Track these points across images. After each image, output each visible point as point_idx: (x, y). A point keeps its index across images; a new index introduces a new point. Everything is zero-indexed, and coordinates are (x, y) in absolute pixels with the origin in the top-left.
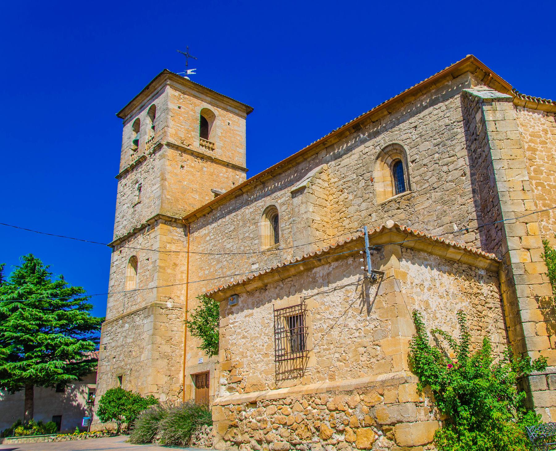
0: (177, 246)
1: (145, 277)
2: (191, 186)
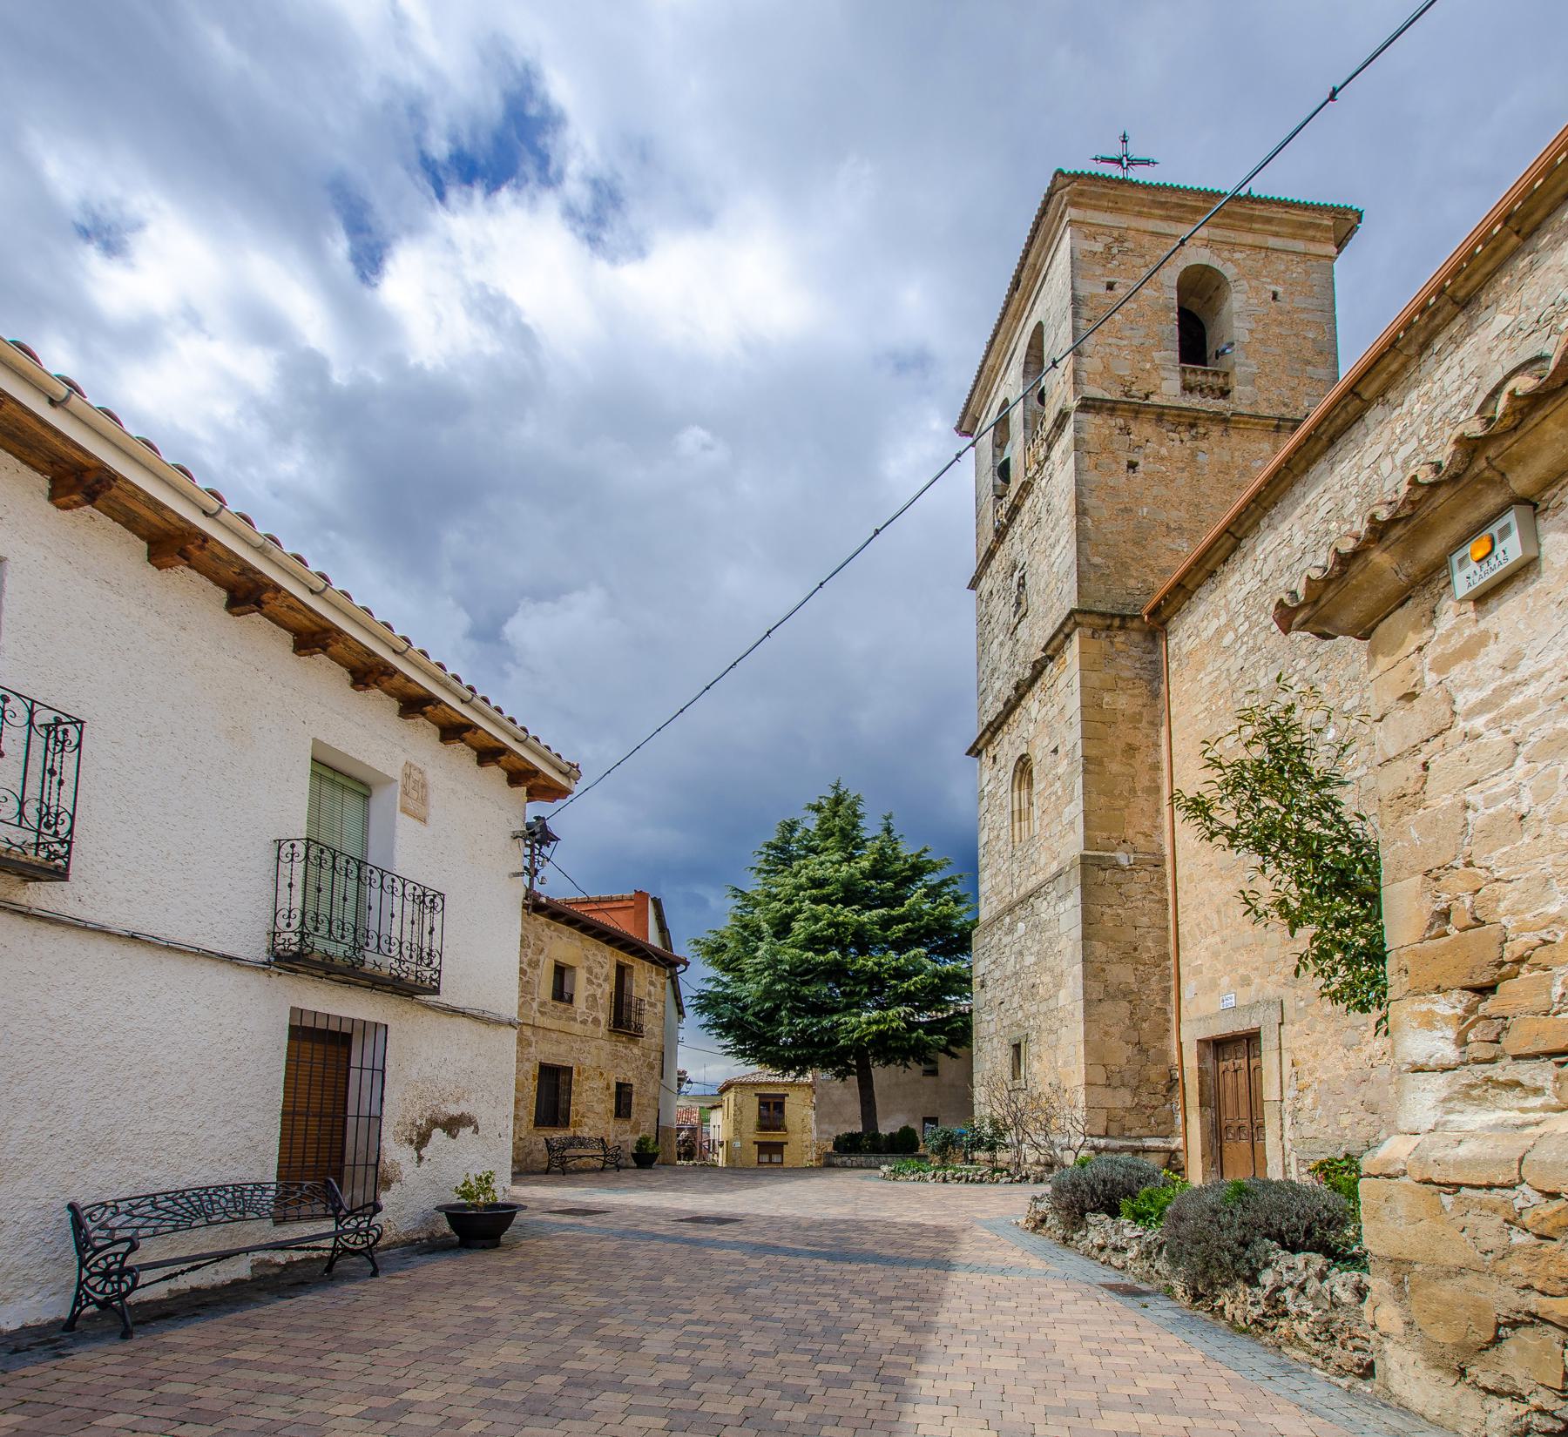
0: (1132, 696)
1: (1053, 798)
2: (1163, 516)
